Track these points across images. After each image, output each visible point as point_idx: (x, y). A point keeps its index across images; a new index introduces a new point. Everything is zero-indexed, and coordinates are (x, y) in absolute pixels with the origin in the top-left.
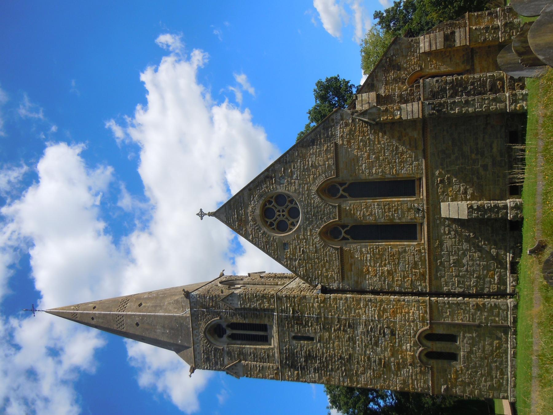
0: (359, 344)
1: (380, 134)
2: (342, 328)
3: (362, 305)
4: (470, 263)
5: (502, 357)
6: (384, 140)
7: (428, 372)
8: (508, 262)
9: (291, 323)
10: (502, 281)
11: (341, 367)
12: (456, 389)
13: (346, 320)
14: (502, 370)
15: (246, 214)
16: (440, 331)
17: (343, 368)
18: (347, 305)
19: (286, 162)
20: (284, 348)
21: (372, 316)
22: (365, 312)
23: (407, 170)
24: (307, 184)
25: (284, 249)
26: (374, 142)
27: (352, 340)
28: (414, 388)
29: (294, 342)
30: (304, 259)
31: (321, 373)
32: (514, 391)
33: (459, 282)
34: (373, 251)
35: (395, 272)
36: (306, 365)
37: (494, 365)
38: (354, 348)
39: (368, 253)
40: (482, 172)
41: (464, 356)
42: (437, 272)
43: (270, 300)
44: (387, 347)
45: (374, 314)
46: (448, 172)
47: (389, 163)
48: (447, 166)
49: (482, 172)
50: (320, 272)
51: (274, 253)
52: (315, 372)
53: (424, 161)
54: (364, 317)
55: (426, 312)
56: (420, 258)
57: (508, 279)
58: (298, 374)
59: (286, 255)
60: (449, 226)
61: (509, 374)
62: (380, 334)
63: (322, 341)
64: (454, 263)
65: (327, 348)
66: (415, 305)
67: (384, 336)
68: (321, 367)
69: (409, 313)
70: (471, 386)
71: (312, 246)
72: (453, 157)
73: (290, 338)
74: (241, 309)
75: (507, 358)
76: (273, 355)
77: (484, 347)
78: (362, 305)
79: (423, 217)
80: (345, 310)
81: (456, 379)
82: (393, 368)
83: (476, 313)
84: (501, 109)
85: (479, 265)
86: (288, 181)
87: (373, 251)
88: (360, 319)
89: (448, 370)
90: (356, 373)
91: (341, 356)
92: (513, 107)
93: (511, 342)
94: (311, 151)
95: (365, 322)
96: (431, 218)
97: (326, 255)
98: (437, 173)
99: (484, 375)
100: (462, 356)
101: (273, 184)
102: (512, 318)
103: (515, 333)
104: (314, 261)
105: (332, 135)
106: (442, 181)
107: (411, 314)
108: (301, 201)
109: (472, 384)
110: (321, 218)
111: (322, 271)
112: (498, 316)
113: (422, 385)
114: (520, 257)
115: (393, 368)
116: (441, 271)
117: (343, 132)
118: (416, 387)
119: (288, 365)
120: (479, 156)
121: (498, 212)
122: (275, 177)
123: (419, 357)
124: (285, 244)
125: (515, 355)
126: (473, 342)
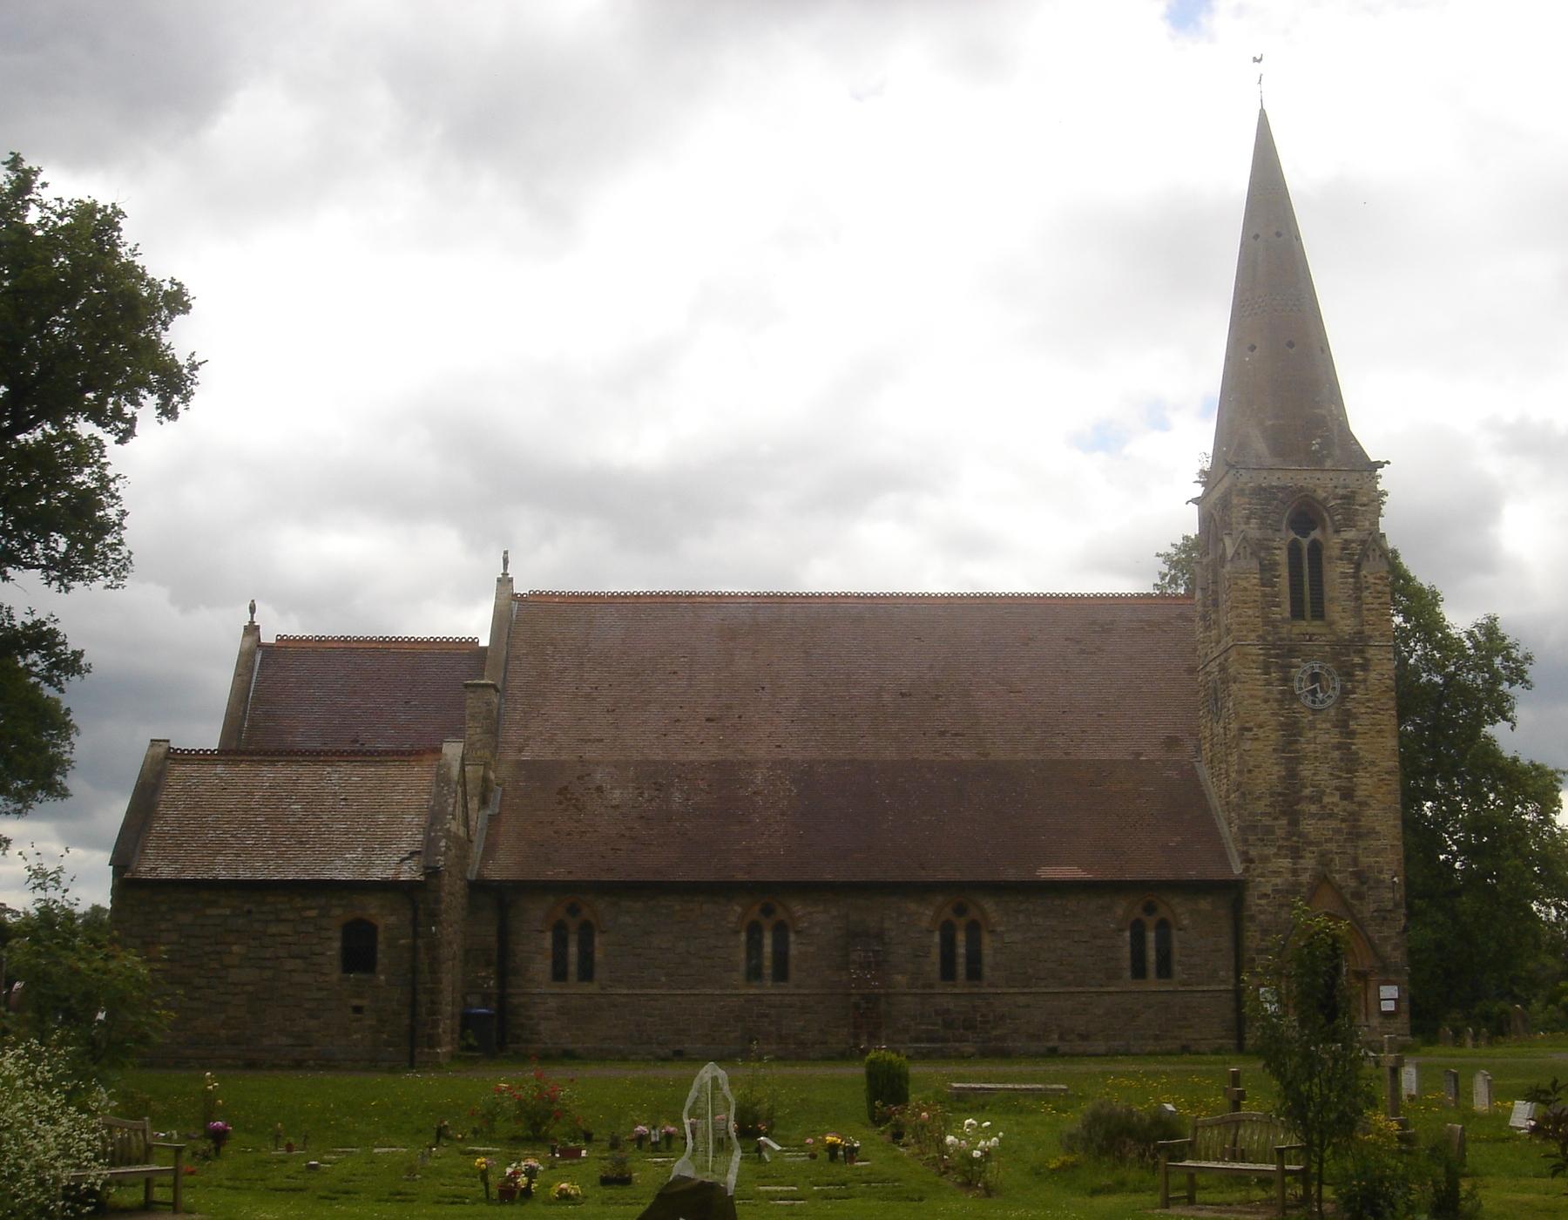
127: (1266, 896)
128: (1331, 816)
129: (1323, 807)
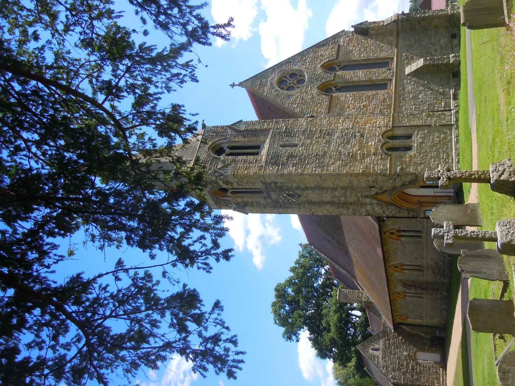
0: (333, 145)
1: (369, 40)
2: (322, 136)
3: (341, 121)
4: (424, 97)
5: (448, 144)
6: (370, 42)
7: (387, 159)
8: (451, 95)
9: (282, 136)
10: (447, 105)
11: (316, 161)
12: (410, 169)
13: (326, 130)
14: (448, 153)
15: (267, 81)
16: (399, 132)
17: (317, 161)
18: (330, 122)
19: (303, 55)
20: (272, 152)
21: (347, 126)
22: (342, 124)
23: (384, 54)
24: (315, 64)
25: (289, 98)
26: (364, 43)
27: (329, 142)
28: (374, 171)
29: (281, 148)
30: (302, 103)
31: (298, 166)
32: (458, 166)
33: (415, 108)
34: (355, 95)
35: (369, 105)
36: (287, 162)
37: (440, 150)
38: (328, 148)
39: (351, 97)
40: (433, 52)
41: (417, 145)
42: (400, 104)
43: (270, 124)
44: (356, 144)
45: (349, 125)
46: (411, 54)
47: (373, 52)
48: (411, 51)
49: (433, 52)
50: (312, 110)
51: (281, 101)
52: (293, 167)
53: (396, 49)
54: (341, 128)
55: (390, 121)
56: (388, 96)
57: (452, 104)
58: (278, 169)
59: (289, 101)
60: (410, 79)
61: (454, 154)
62: (352, 136)
63: (304, 146)
64: (412, 97)
65: (307, 150)
66: (381, 118)
67: (355, 138)
68: (299, 162)
69: (376, 122)
70: (423, 165)
71: (310, 95)
72: (415, 47)
73: (279, 145)
74: (244, 131)
75: (452, 145)
76: (261, 160)
77: (433, 139)
78: (341, 121)
79: (393, 75)
80: (327, 125)
81: (410, 162)
82: (359, 158)
83: (427, 119)
84: (445, 14)
85: (431, 98)
86: (302, 63)
87: (355, 95)
88: (338, 129)
89: (404, 157)
90: (327, 164)
91: (317, 154)
92: (452, 12)
93: (454, 134)
94: (322, 49)
95: (341, 131)
96: (398, 76)
97: (319, 99)
98: (404, 54)
99: (433, 157)
100: (415, 145)
101: (291, 65)
102: (455, 119)
103: (457, 128)
104: (309, 104)
105: (337, 41)
106: (407, 58)
107: (378, 123)
108: (307, 73)
109: (424, 164)
110: (320, 80)
111: (314, 109)
112: (444, 120)
113: (381, 167)
114: (460, 89)
115: (359, 158)
116: (403, 102)
117: (345, 40)
118: (376, 170)
119: (272, 163)
120: (432, 46)
121: (443, 60)
122: (293, 62)
123: (381, 148)
124: (290, 96)
125: (457, 142)
126: (424, 136)
127: (384, 212)
128: (345, 194)
129: (342, 196)
